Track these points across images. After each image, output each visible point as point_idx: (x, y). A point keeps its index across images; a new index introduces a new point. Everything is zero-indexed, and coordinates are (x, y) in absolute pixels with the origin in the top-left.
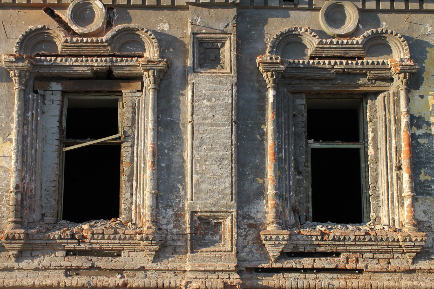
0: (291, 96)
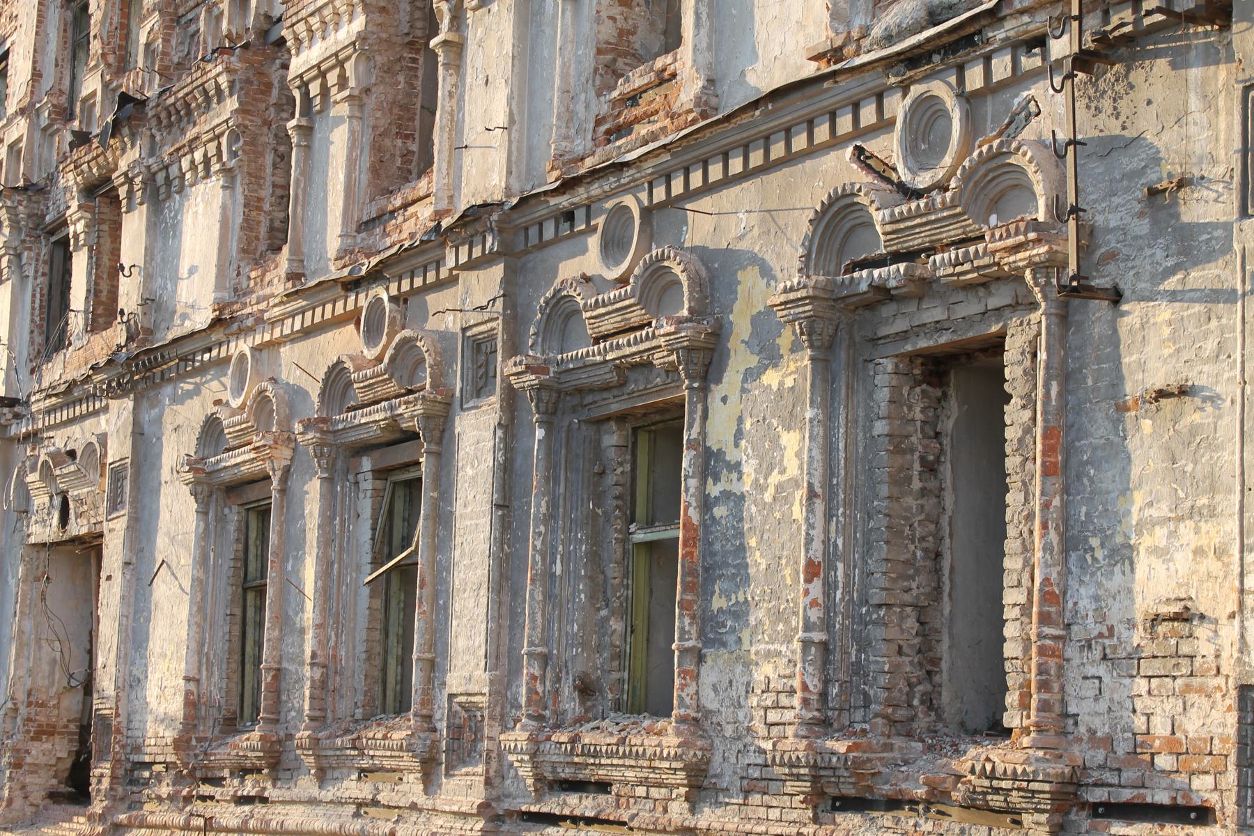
0: (587, 431)
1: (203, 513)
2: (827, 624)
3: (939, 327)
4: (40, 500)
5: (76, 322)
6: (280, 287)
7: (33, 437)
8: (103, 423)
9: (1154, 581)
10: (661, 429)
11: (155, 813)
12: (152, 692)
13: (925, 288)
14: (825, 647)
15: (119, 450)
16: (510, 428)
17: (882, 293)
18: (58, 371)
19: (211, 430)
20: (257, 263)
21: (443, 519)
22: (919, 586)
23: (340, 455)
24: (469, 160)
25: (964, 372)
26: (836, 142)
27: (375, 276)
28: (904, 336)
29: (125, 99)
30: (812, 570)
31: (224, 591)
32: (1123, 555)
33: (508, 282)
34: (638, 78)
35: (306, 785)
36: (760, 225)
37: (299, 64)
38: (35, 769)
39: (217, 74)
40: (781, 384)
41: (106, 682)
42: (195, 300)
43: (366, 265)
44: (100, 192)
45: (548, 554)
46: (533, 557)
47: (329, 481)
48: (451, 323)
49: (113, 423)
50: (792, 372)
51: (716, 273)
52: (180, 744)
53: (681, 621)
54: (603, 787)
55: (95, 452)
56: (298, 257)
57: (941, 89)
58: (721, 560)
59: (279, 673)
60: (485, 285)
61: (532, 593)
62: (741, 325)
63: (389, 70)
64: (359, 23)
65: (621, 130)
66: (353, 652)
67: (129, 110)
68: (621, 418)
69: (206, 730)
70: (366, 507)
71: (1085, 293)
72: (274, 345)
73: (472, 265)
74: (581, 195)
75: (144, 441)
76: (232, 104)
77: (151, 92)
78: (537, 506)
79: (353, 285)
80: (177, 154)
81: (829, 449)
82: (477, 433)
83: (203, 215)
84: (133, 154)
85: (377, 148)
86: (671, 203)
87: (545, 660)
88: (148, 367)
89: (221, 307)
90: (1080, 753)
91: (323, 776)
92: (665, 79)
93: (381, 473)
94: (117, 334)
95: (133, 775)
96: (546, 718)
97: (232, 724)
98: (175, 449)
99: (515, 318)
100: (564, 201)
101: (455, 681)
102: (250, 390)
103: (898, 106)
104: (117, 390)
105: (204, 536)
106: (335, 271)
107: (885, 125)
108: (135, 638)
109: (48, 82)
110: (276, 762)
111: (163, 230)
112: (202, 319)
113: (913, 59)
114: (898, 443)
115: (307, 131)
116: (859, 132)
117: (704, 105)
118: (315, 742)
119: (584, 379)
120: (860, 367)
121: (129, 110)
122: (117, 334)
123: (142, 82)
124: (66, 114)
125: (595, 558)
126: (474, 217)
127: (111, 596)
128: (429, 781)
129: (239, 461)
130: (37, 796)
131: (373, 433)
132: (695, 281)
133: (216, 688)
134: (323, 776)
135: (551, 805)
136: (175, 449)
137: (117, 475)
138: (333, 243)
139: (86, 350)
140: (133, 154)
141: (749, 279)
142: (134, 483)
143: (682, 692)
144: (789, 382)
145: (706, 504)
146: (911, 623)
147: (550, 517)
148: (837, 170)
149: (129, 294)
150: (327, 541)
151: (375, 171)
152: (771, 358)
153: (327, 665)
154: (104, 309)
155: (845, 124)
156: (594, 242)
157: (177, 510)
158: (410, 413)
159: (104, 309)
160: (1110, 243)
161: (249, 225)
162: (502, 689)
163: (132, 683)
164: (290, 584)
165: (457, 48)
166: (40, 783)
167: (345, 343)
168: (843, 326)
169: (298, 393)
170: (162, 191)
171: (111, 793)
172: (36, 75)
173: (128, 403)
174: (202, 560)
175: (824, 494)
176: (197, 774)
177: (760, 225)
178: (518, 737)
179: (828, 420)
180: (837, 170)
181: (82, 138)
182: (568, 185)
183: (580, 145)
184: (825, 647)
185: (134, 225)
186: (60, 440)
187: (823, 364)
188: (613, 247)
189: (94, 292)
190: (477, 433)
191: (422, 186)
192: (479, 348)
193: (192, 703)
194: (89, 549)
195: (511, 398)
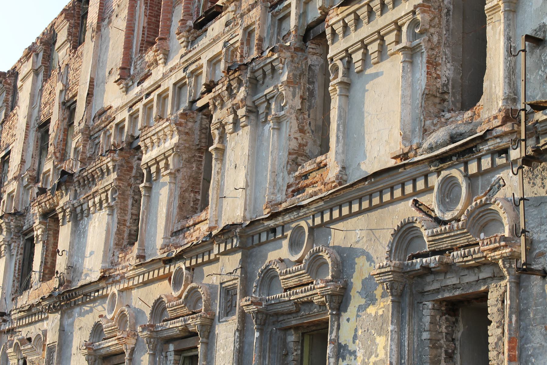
3: (455, 287)
5: (35, 277)
6: (134, 262)
7: (11, 331)
8: (45, 325)
13: (448, 268)
15: (52, 338)
16: (242, 332)
17: (427, 270)
18: (24, 300)
19: (97, 329)
20: (122, 250)
24: (226, 204)
25: (468, 310)
26: (404, 197)
27: (179, 257)
28: (438, 291)
29: (64, 173)
33: (243, 261)
34: (308, 166)
36: (366, 238)
37: (146, 158)
39: (108, 162)
40: (376, 313)
42: (92, 267)
43: (175, 252)
44: (50, 217)
47: (153, 355)
48: (215, 281)
49: (51, 324)
50: (383, 307)
51: (345, 259)
56: (142, 248)
57: (457, 173)
62: (357, 284)
63: (189, 161)
64: (176, 139)
67: (65, 179)
68: (296, 328)
73: (226, 253)
74: (280, 220)
75: (64, 334)
77: (76, 170)
79: (168, 261)
80: (87, 199)
81: (400, 345)
82: (226, 333)
83: (98, 228)
84: (66, 199)
86: (324, 225)
88: (68, 299)
92: (321, 167)
93: (178, 352)
94: (54, 283)
98: (80, 337)
99: (246, 279)
102: (117, 311)
103: (435, 181)
104: (53, 309)
106: (160, 255)
107: (428, 190)
109: (28, 165)
111: (78, 233)
112: (95, 276)
113: (443, 159)
114: (434, 343)
115: (149, 189)
116: (416, 193)
117: (340, 180)
119: (279, 308)
121: (65, 179)
122: (54, 283)
123: (72, 165)
124: (35, 180)
126: (228, 230)
129: (110, 345)
131: (176, 332)
132: (335, 263)
136: (80, 337)
137: (51, 351)
138: (159, 241)
139: (39, 290)
140: (66, 199)
144: (380, 312)
148: (405, 211)
151: (180, 208)
152: (371, 300)
154: (49, 271)
155: (409, 189)
156: (285, 243)
158: (194, 323)
159: (49, 271)
161: (119, 232)
165: (222, 151)
167: (163, 289)
168: (408, 286)
169: (139, 312)
170: (78, 216)
172: (23, 162)
173: (58, 316)
179: (400, 331)
180: (405, 211)
181: (42, 191)
182: (274, 216)
183: (280, 197)
185: (65, 232)
186: (24, 333)
187: (398, 304)
188: (294, 245)
189: (44, 263)
190: (226, 333)
191: (203, 215)
192: (228, 293)
195: (243, 317)
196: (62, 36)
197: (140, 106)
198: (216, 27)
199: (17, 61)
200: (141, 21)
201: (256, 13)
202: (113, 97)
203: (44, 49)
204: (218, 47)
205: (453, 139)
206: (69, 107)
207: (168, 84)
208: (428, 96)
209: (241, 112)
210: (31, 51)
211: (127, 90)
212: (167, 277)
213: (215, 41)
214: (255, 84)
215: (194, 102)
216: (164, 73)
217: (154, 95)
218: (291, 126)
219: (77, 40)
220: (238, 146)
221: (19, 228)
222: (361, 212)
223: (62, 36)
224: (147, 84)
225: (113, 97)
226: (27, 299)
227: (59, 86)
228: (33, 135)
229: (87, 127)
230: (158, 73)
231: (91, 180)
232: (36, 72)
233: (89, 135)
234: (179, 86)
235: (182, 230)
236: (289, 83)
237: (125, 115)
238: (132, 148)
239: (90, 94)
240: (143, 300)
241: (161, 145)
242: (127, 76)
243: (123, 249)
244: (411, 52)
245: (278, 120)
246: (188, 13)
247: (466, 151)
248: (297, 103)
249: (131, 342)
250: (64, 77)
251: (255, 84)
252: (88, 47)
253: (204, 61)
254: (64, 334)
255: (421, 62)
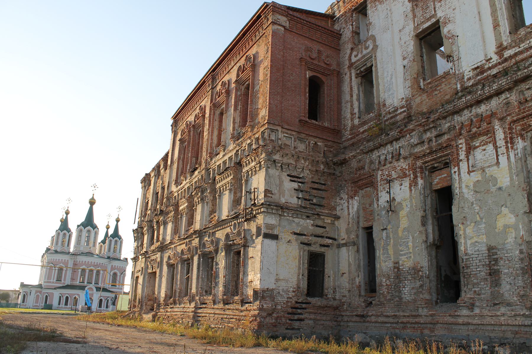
1: (168, 269)
2: (225, 283)
4: (149, 266)
5: (155, 241)
6: (177, 238)
7: (149, 257)
8: (158, 256)
9: (250, 278)
10: (213, 258)
11: (161, 310)
12: (162, 294)
13: (234, 244)
14: (225, 286)
15: (159, 260)
16: (199, 259)
17: (231, 245)
18: (153, 248)
19: (169, 258)
21: (192, 270)
22: (235, 279)
23: (183, 261)
25: (239, 253)
26: (228, 226)
27: (186, 238)
30: (224, 277)
31: (170, 280)
32: (248, 275)
33: (199, 240)
35: (178, 306)
37: (181, 208)
38: (148, 305)
39: (171, 208)
41: (156, 293)
42: (168, 238)
44: (158, 222)
45: (202, 275)
46: (201, 275)
47: (181, 265)
48: (194, 245)
49: (158, 255)
50: (223, 254)
51: (218, 240)
52: (164, 301)
53: (213, 283)
54: (206, 303)
55: (155, 260)
56: (179, 234)
57: (236, 222)
58: (217, 276)
59: (175, 291)
60: (197, 240)
61: (200, 280)
62: (220, 248)
63: (190, 210)
64: (187, 204)
65: (211, 222)
66: (183, 288)
69: (168, 299)
70: (186, 268)
71: (245, 246)
72: (176, 246)
73: (196, 238)
74: (206, 230)
75: (162, 258)
76: (173, 212)
78: (201, 269)
79: (184, 239)
80: (167, 219)
82: (196, 259)
83: (170, 226)
84: (162, 218)
85: (188, 221)
86: (214, 232)
87: (201, 288)
88: (162, 248)
89: (171, 240)
90: (244, 297)
91: (180, 304)
94: (159, 243)
95: (159, 305)
96: (202, 295)
97: (171, 298)
98: (165, 260)
100: (204, 231)
101: (192, 291)
102: (173, 252)
103: (233, 223)
105: (168, 272)
108: (160, 286)
109: (153, 206)
110: (175, 303)
111: (165, 229)
112: (168, 243)
113: (233, 218)
114: (233, 262)
115: (181, 217)
118: (178, 300)
120: (230, 253)
122: (159, 243)
123: (163, 208)
124: (155, 210)
125: (208, 275)
126: (195, 232)
127: (157, 280)
128: (190, 304)
130: (149, 309)
131: (186, 259)
132: (216, 242)
133: (169, 293)
134: (180, 304)
135: (201, 306)
136: (165, 260)
137: (158, 263)
139: (156, 245)
140: (162, 218)
141: (221, 241)
142: (160, 264)
143: (213, 292)
145: (216, 269)
146: (234, 283)
147: (202, 270)
148: (228, 230)
149: (161, 239)
150: (181, 273)
151: (188, 224)
152: (222, 252)
153: (181, 290)
154: (158, 240)
157: (165, 268)
159: (158, 240)
160: (248, 241)
161: (175, 229)
162: (197, 292)
163: (159, 292)
164: (177, 279)
165: (196, 209)
166: (149, 308)
167: (183, 246)
168: (228, 248)
169: (179, 252)
170: (165, 223)
171: (156, 308)
172: (152, 204)
174: (168, 275)
175: (226, 268)
176: (166, 305)
177: (220, 235)
178: (197, 298)
179: (226, 259)
180: (228, 230)
181: (156, 215)
182: (204, 229)
183: (207, 223)
184: (225, 286)
185: (162, 228)
186: (152, 258)
188: (209, 237)
190: (196, 259)
192: (196, 248)
193: (166, 295)
194: (155, 273)
195: (199, 255)
196: (162, 167)
197: (180, 192)
198: (196, 173)
199: (151, 169)
200: (181, 166)
201: (204, 171)
202: (174, 188)
203: (157, 169)
204: (196, 179)
205: (235, 213)
206: (163, 188)
207: (186, 187)
208: (234, 201)
209: (199, 199)
210: (154, 169)
211: (177, 187)
212: (184, 243)
213: (196, 177)
214: (203, 192)
215: (192, 193)
216: (185, 184)
217: (183, 190)
218: (210, 204)
219: (166, 169)
220: (199, 208)
221: (151, 225)
222: (221, 229)
223: (162, 167)
224: (181, 186)
225: (174, 188)
226: (153, 248)
227: (161, 182)
228: (154, 196)
229: (167, 196)
230: (184, 182)
231: (168, 213)
232: (155, 176)
233: (168, 199)
234: (189, 188)
235: (189, 230)
236: (209, 193)
237: (176, 194)
238: (177, 206)
239: (168, 186)
240: (179, 249)
241: (183, 206)
242: (177, 183)
243: (176, 234)
244: (230, 190)
245: (207, 203)
246: (190, 167)
247: (236, 217)
248: (212, 198)
249: (177, 261)
250: (162, 179)
251: (203, 192)
252: (168, 171)
253: (193, 182)
254: (162, 258)
255: (233, 192)
